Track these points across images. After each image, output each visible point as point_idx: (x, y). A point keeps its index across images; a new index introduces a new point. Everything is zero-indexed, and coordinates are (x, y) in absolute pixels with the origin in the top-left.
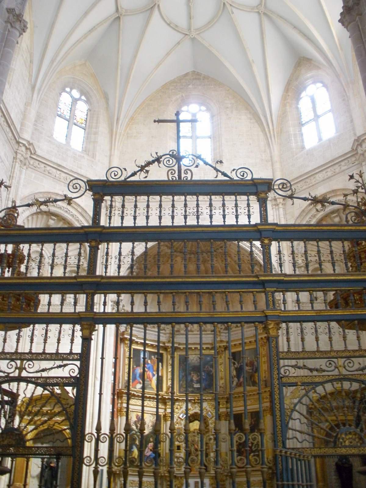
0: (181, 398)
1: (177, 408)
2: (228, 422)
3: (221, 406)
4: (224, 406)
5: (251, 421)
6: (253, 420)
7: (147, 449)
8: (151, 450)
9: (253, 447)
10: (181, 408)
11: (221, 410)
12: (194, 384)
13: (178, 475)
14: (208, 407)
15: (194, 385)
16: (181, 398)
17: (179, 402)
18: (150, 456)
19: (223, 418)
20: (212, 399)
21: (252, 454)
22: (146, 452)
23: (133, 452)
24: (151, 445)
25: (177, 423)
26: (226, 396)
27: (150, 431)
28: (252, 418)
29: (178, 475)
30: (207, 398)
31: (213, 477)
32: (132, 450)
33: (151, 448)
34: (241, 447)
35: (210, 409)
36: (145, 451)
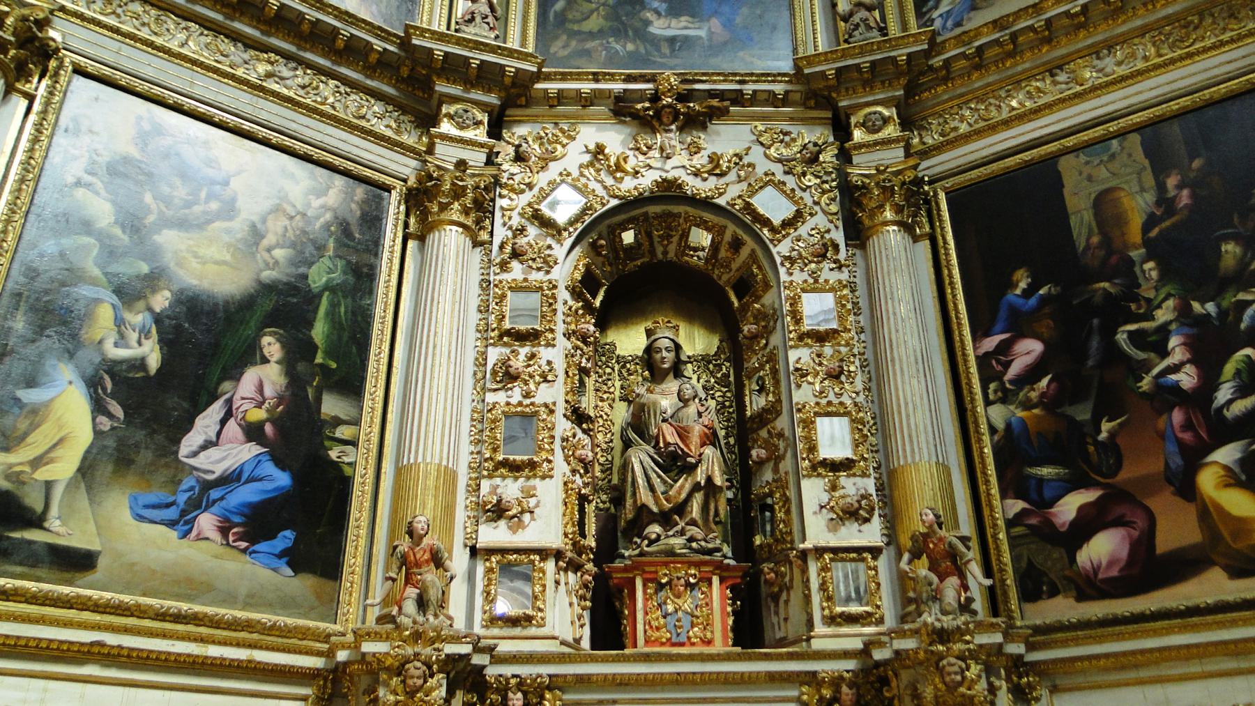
0: (553, 86)
1: (519, 158)
2: (926, 243)
3: (858, 135)
4: (891, 131)
5: (1161, 187)
6: (1172, 182)
7: (215, 411)
8: (253, 432)
9: (1224, 393)
10: (547, 159)
11: (862, 167)
12: (649, 15)
13: (508, 670)
14: (757, 151)
15: (648, 23)
16: (553, 86)
17: (533, 119)
18: (230, 479)
19: (889, 214)
20: (785, 100)
21: (1227, 454)
22: (191, 441)
23: (36, 414)
24: (262, 382)
25: (516, 254)
26: (901, 54)
27: (268, 275)
28: (1160, 160)
29: (508, 670)
30: (749, 88)
31: (836, 682)
32: (29, 396)
33: (257, 415)
34: (1082, 413)
35: (778, 169)
36: (186, 424)
